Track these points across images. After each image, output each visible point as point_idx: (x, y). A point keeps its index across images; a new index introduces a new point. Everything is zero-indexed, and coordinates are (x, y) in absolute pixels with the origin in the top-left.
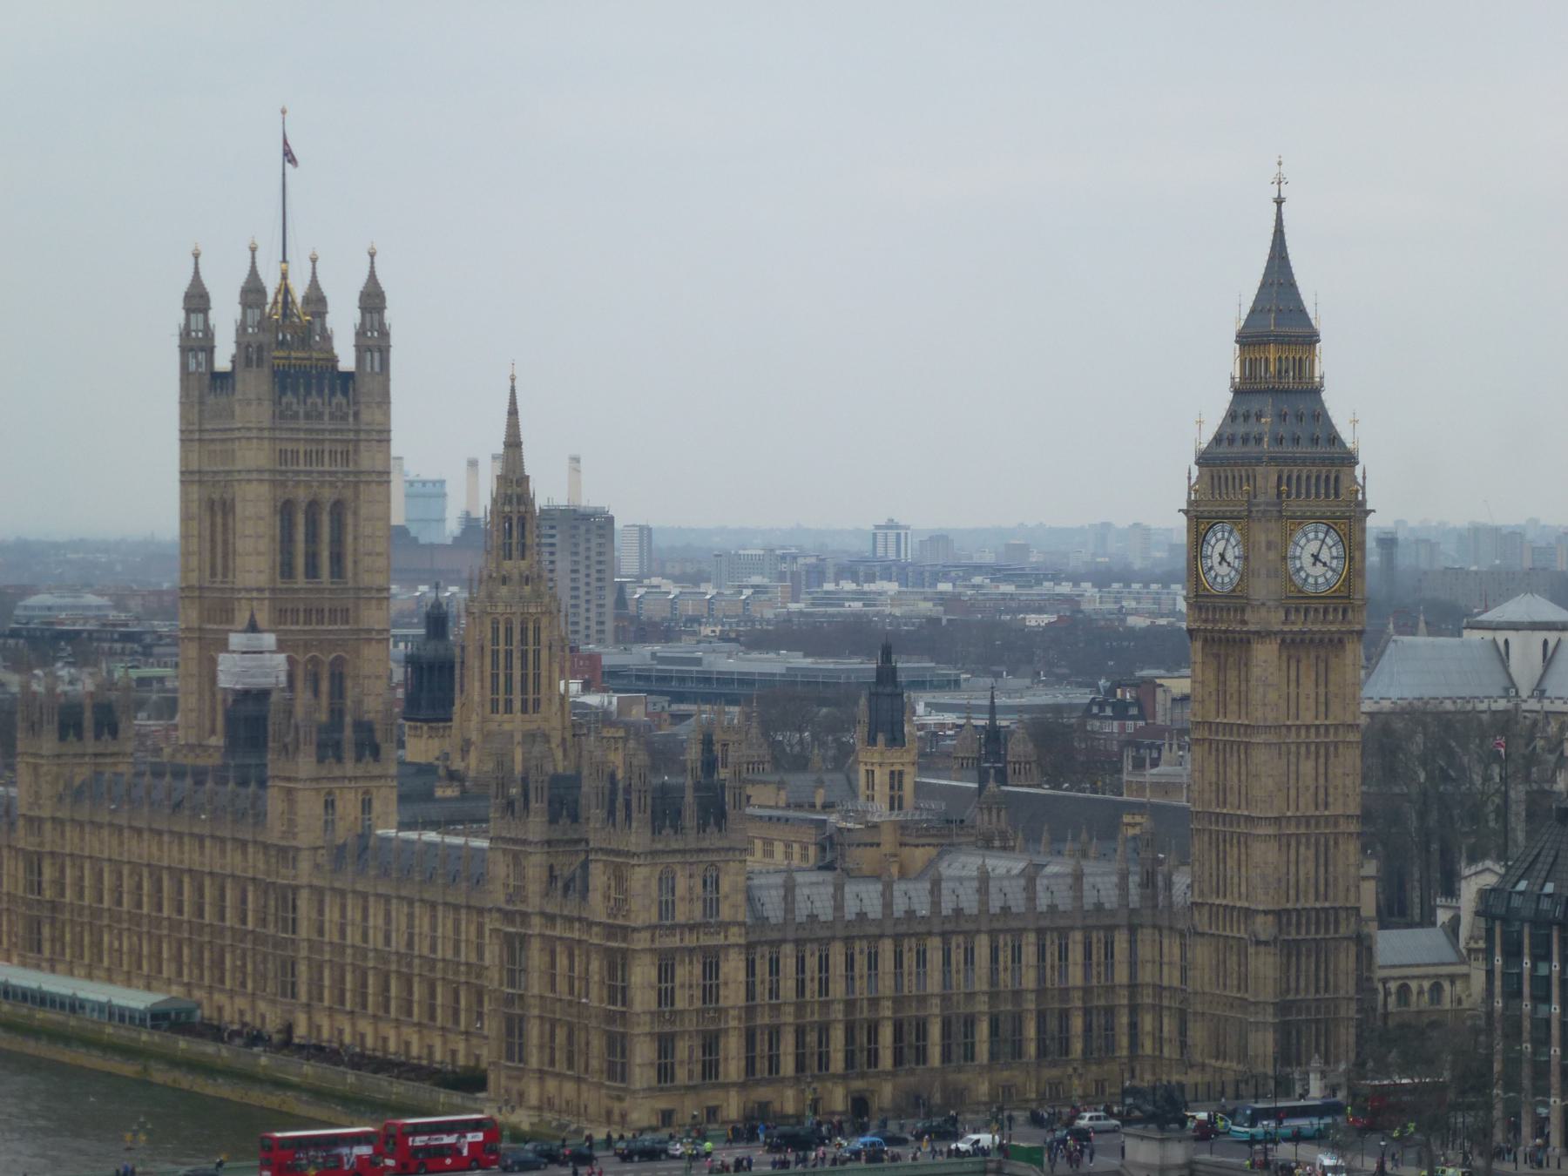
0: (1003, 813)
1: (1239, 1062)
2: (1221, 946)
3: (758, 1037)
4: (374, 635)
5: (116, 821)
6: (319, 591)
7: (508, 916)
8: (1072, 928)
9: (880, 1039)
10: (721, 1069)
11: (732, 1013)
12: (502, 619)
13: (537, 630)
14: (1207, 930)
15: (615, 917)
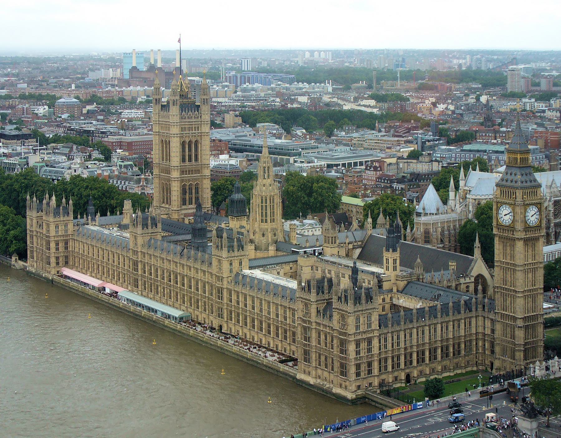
0: (422, 268)
1: (511, 359)
2: (505, 325)
3: (382, 361)
4: (206, 177)
5: (161, 256)
6: (192, 165)
7: (304, 321)
8: (461, 319)
9: (413, 357)
10: (372, 371)
11: (375, 355)
12: (264, 197)
13: (273, 199)
14: (500, 320)
15: (343, 329)
